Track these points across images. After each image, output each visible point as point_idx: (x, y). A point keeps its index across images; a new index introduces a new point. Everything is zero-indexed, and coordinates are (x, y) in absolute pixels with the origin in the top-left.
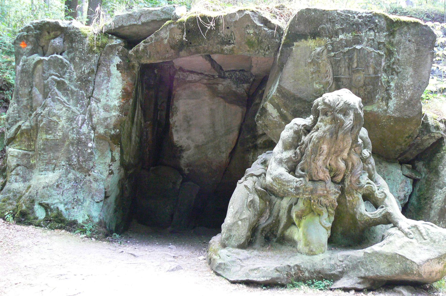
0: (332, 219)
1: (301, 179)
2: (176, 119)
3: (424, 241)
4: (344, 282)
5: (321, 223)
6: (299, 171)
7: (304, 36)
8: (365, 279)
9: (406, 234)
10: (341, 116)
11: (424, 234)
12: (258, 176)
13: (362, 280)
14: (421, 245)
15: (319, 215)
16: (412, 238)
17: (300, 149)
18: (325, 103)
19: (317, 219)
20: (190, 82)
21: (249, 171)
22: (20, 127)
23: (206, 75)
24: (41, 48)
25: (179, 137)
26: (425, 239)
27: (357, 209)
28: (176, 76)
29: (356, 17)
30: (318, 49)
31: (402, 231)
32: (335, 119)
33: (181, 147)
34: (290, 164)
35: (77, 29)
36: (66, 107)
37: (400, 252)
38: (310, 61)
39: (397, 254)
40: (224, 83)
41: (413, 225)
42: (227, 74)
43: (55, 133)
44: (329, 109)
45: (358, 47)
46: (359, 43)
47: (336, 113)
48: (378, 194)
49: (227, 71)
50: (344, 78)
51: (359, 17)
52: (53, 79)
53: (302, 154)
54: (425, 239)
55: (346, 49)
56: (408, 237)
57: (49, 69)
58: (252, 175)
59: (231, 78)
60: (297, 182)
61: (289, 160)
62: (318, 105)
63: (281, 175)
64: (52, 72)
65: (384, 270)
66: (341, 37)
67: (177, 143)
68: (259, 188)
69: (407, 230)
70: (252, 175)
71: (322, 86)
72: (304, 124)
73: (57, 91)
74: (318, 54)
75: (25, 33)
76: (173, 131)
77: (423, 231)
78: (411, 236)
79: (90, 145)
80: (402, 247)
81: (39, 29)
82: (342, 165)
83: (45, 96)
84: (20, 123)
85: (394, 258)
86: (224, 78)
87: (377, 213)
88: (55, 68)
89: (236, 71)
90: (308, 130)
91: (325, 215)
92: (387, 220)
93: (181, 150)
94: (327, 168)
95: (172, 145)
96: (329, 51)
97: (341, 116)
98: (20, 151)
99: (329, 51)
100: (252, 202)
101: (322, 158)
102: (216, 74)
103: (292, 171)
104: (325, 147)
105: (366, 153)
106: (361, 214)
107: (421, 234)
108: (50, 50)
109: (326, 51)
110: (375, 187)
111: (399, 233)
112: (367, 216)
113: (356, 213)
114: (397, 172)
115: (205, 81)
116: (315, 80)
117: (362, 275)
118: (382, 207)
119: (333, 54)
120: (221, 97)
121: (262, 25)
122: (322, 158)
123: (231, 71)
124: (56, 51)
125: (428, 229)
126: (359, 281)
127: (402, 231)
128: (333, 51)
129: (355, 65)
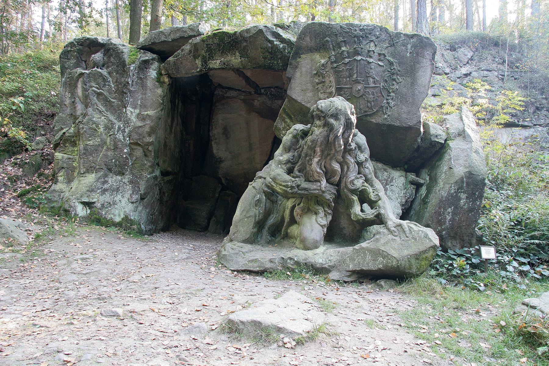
0: (330, 218)
1: (297, 179)
2: (216, 131)
4: (334, 275)
5: (316, 221)
6: (296, 172)
7: (311, 50)
8: (354, 272)
9: (391, 232)
10: (332, 121)
11: (408, 232)
14: (403, 242)
18: (318, 109)
19: (314, 217)
20: (228, 97)
21: (259, 174)
22: (64, 133)
23: (244, 92)
24: (84, 63)
25: (218, 149)
26: (407, 237)
28: (215, 93)
29: (357, 29)
30: (323, 61)
31: (389, 229)
32: (327, 124)
33: (219, 158)
34: (289, 165)
35: (115, 45)
36: (104, 116)
37: (382, 248)
38: (315, 72)
40: (259, 99)
42: (263, 91)
43: (95, 139)
44: (322, 115)
45: (359, 58)
46: (359, 54)
48: (372, 197)
49: (263, 88)
50: (346, 88)
51: (361, 30)
52: (93, 90)
53: (300, 156)
54: (407, 237)
55: (347, 60)
57: (90, 81)
58: (261, 177)
61: (288, 162)
62: (313, 111)
63: (278, 175)
64: (93, 84)
65: (371, 264)
66: (343, 49)
67: (216, 155)
70: (261, 177)
72: (301, 129)
73: (96, 101)
74: (323, 65)
75: (69, 49)
76: (213, 143)
77: (407, 229)
78: (396, 234)
79: (125, 151)
80: (386, 243)
81: (81, 45)
82: (337, 167)
83: (86, 106)
84: (64, 131)
85: (376, 253)
86: (260, 94)
87: (369, 213)
88: (95, 80)
90: (305, 134)
91: (322, 214)
92: (379, 220)
93: (220, 161)
94: (321, 169)
95: (212, 155)
96: (332, 63)
97: (332, 121)
98: (65, 155)
99: (332, 63)
100: (259, 201)
101: (316, 160)
102: (253, 91)
103: (290, 172)
104: (318, 149)
105: (364, 156)
106: (355, 214)
107: (404, 232)
108: (91, 64)
109: (329, 63)
110: (370, 190)
111: (386, 231)
114: (399, 179)
115: (243, 97)
118: (376, 209)
119: (335, 65)
120: (257, 112)
121: (275, 40)
122: (316, 160)
123: (267, 88)
124: (96, 65)
126: (348, 274)
127: (389, 229)
128: (335, 62)
129: (355, 76)
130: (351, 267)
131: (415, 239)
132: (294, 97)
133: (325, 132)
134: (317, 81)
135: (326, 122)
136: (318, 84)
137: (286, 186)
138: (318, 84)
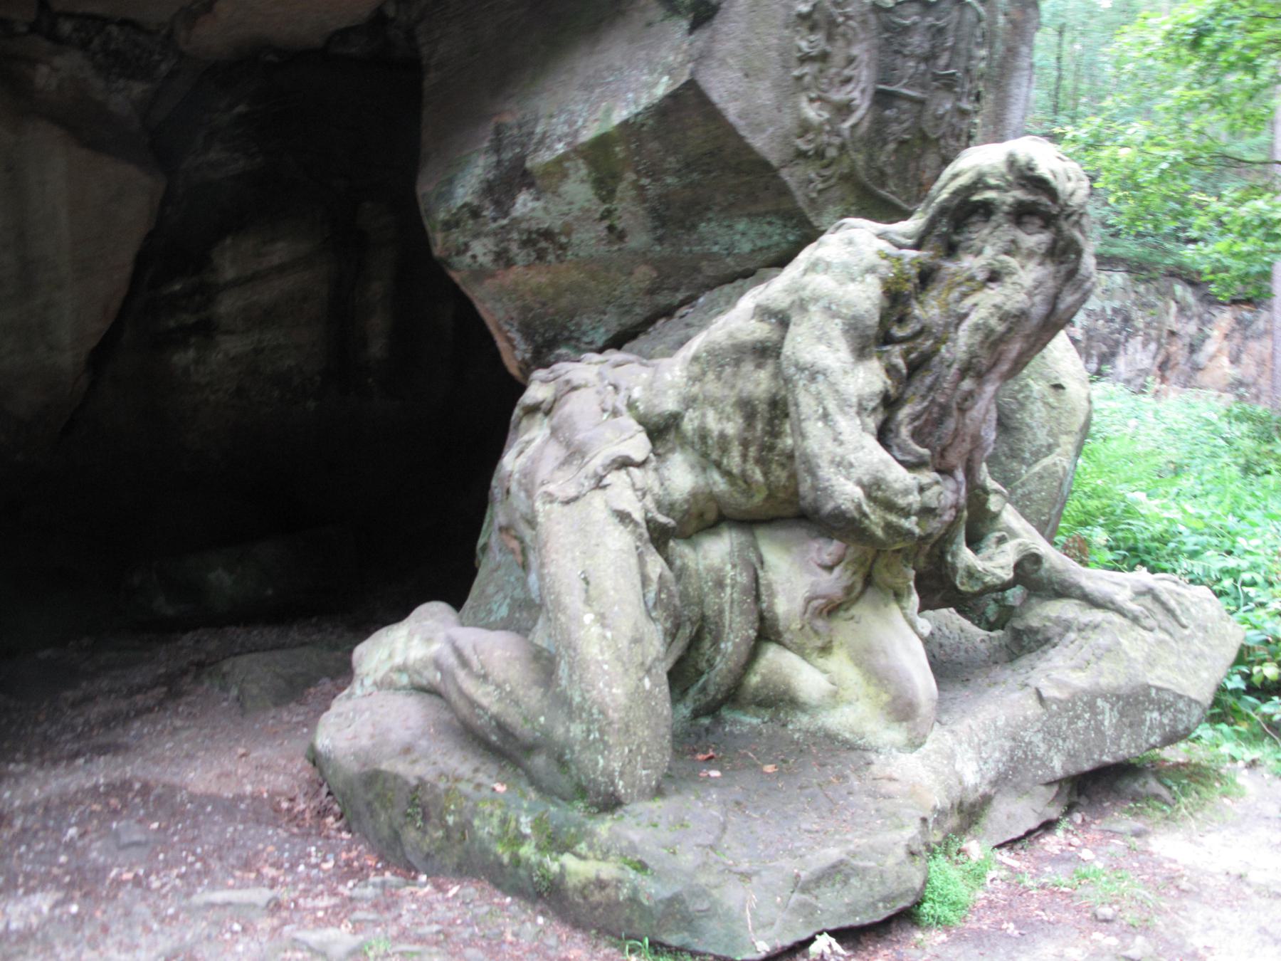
3: (1187, 632)
9: (1135, 620)
11: (1178, 612)
12: (641, 465)
13: (1055, 789)
15: (898, 596)
16: (1151, 630)
17: (906, 354)
26: (1184, 627)
27: (954, 555)
31: (1120, 611)
39: (1150, 686)
40: (58, 61)
41: (1144, 589)
42: (66, 27)
47: (1065, 226)
49: (70, 16)
54: (1184, 627)
56: (1145, 628)
58: (624, 463)
59: (84, 46)
60: (922, 489)
62: (979, 183)
68: (662, 519)
69: (1134, 607)
70: (624, 463)
71: (826, 115)
78: (1149, 622)
80: (1151, 662)
89: (105, 21)
111: (1116, 618)
112: (994, 574)
113: (954, 569)
116: (806, 89)
117: (1059, 773)
118: (1001, 540)
125: (1178, 594)
127: (1120, 611)
130: (1058, 766)
131: (1205, 630)
132: (715, 97)
133: (1050, 283)
134: (804, 45)
135: (1055, 242)
136: (805, 59)
137: (905, 513)
138: (805, 59)
